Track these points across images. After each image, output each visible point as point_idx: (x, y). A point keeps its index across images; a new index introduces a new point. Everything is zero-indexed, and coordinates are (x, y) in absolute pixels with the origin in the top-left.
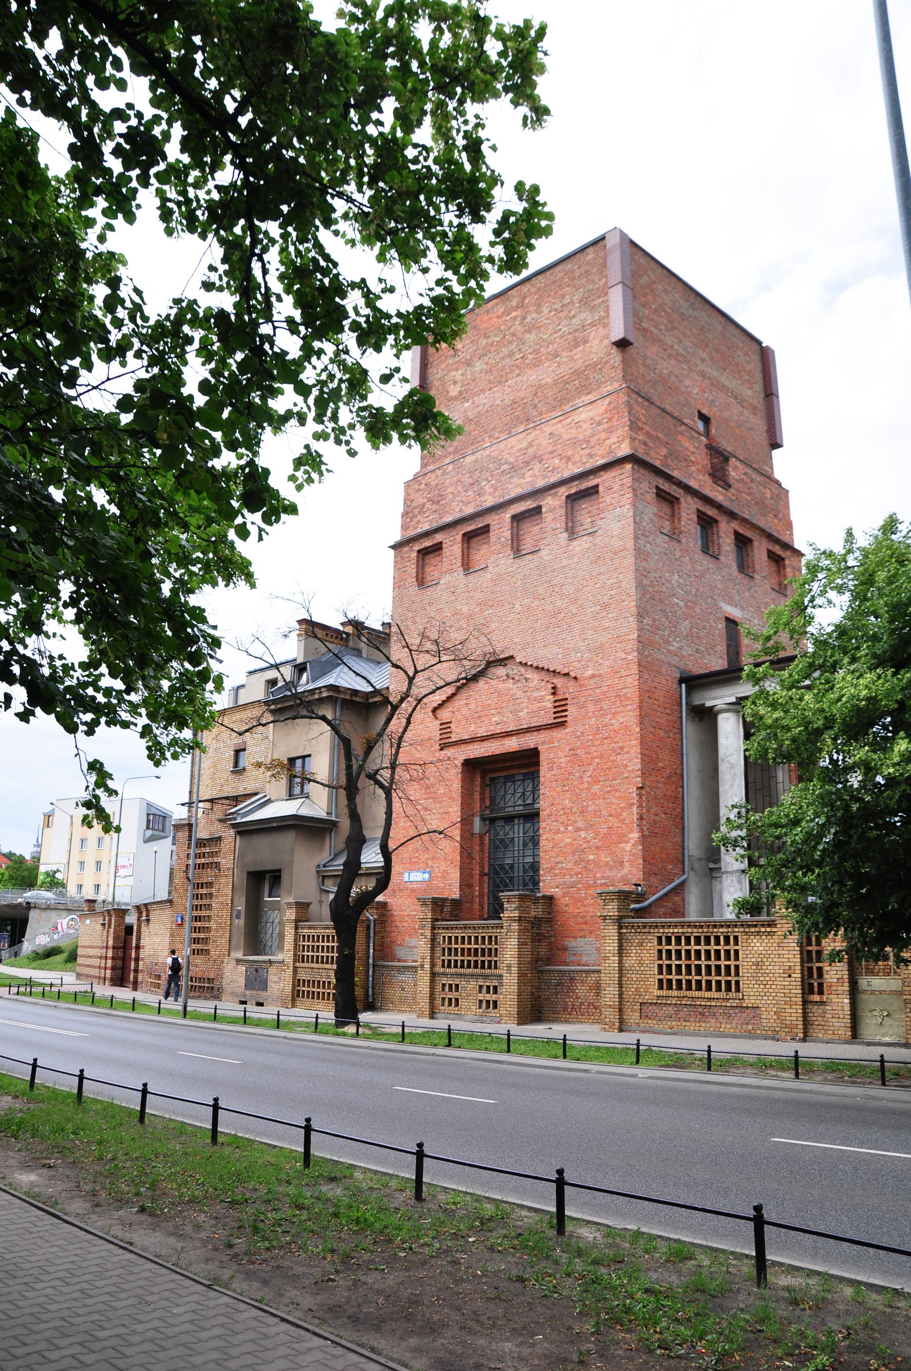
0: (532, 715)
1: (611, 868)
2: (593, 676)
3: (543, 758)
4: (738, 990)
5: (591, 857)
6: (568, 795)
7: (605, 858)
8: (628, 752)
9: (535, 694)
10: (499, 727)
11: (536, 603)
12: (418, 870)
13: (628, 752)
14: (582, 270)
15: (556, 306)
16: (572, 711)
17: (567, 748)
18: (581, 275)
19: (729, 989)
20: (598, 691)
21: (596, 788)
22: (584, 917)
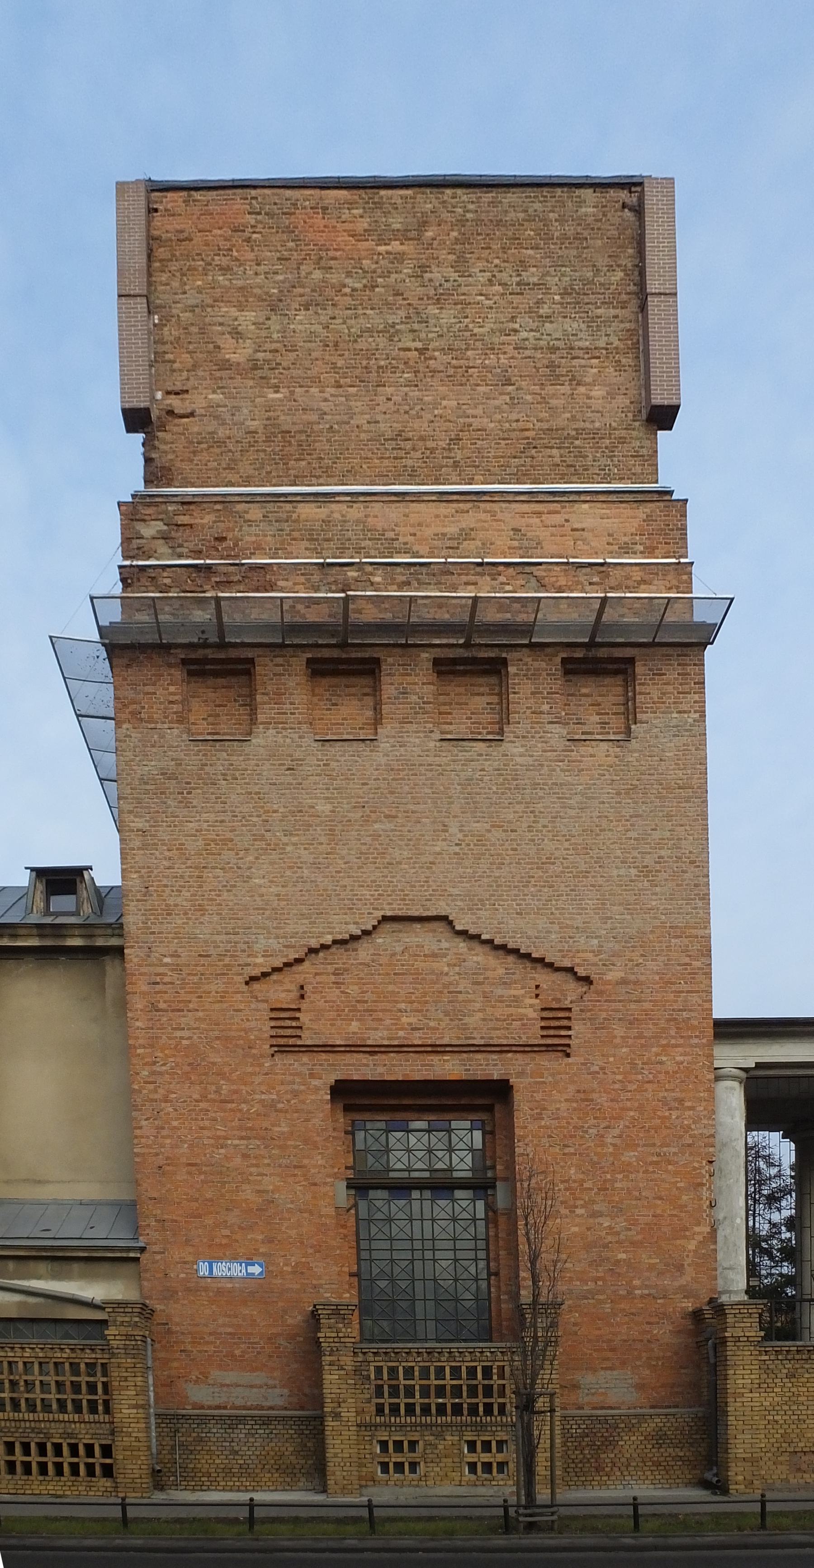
0: (491, 1025)
1: (661, 1274)
2: (624, 982)
3: (520, 1098)
4: (107, 1410)
5: (622, 1256)
6: (575, 1160)
7: (647, 1258)
8: (692, 1108)
9: (499, 991)
10: (417, 1034)
11: (497, 834)
12: (234, 1258)
13: (692, 1108)
14: (570, 229)
15: (504, 276)
16: (579, 1030)
17: (572, 1088)
18: (564, 237)
19: (93, 1409)
20: (633, 1006)
21: (629, 1156)
22: (610, 1341)
